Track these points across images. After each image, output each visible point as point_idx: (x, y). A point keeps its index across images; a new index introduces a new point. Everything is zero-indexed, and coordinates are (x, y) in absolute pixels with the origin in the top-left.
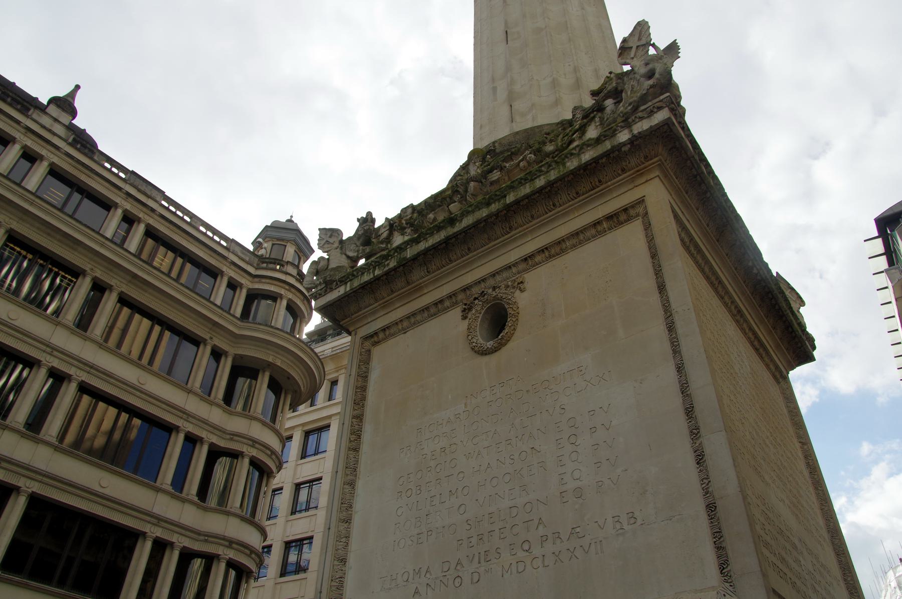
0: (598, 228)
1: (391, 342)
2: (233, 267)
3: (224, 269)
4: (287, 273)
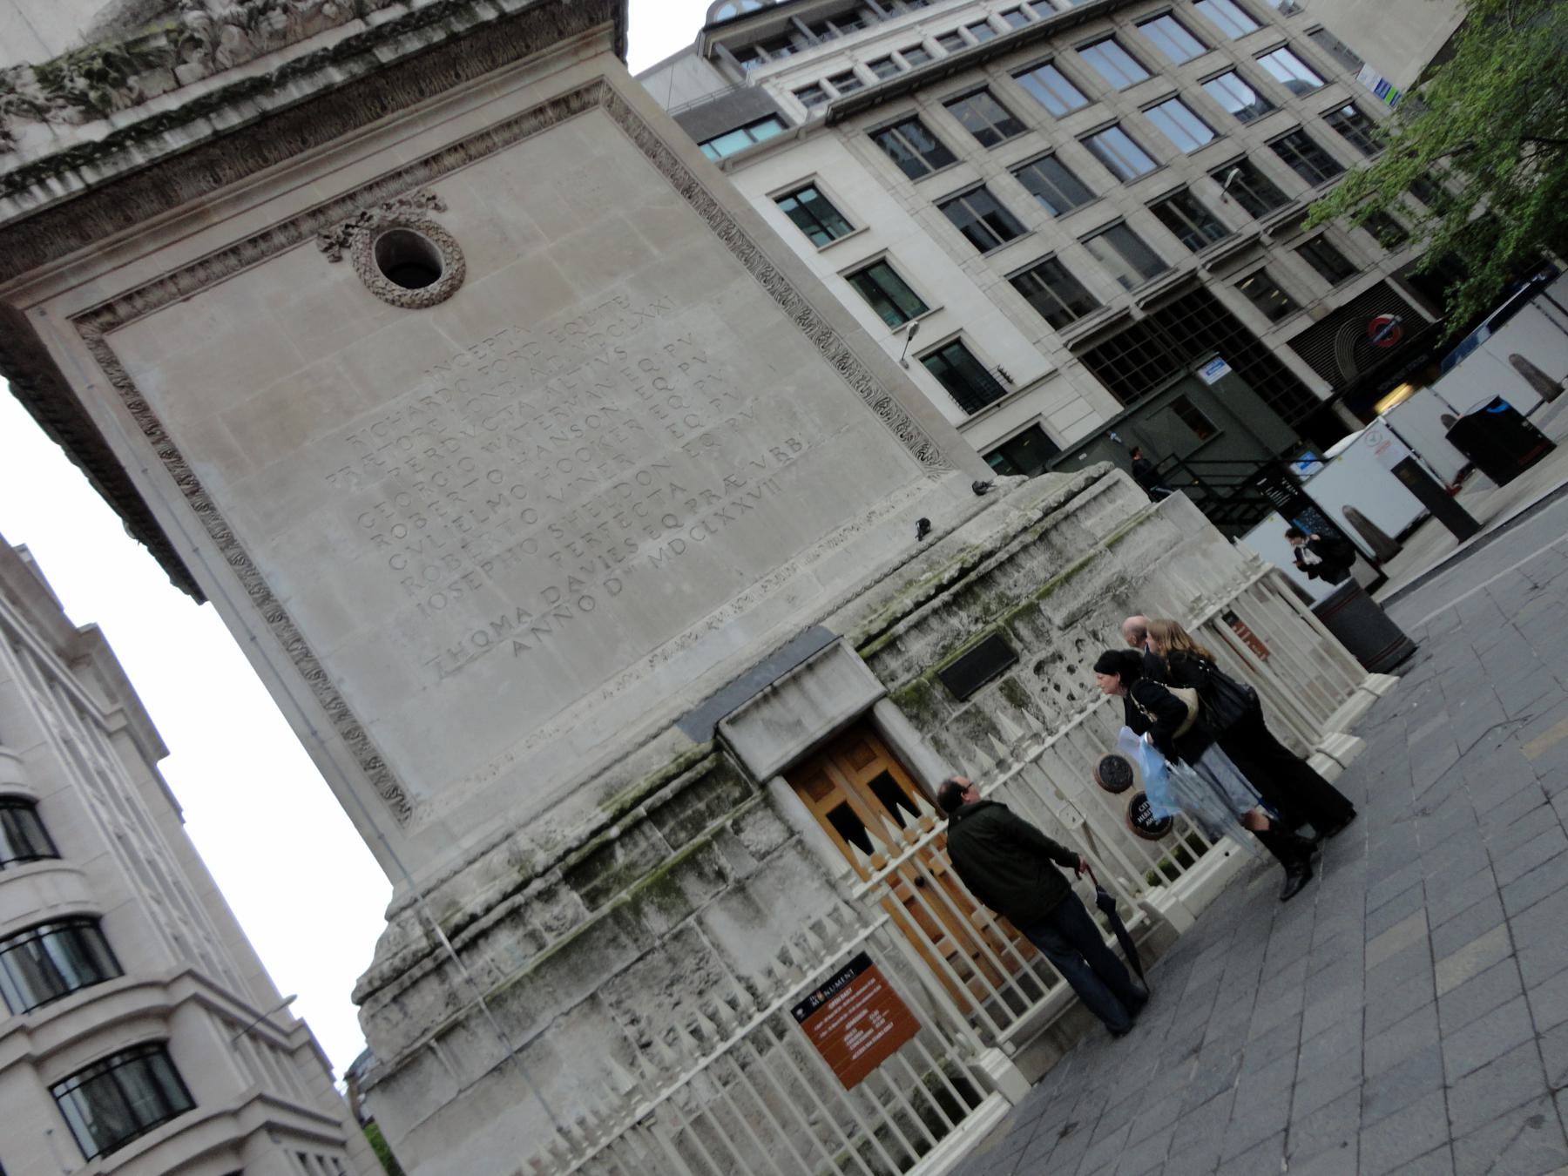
1: (153, 321)
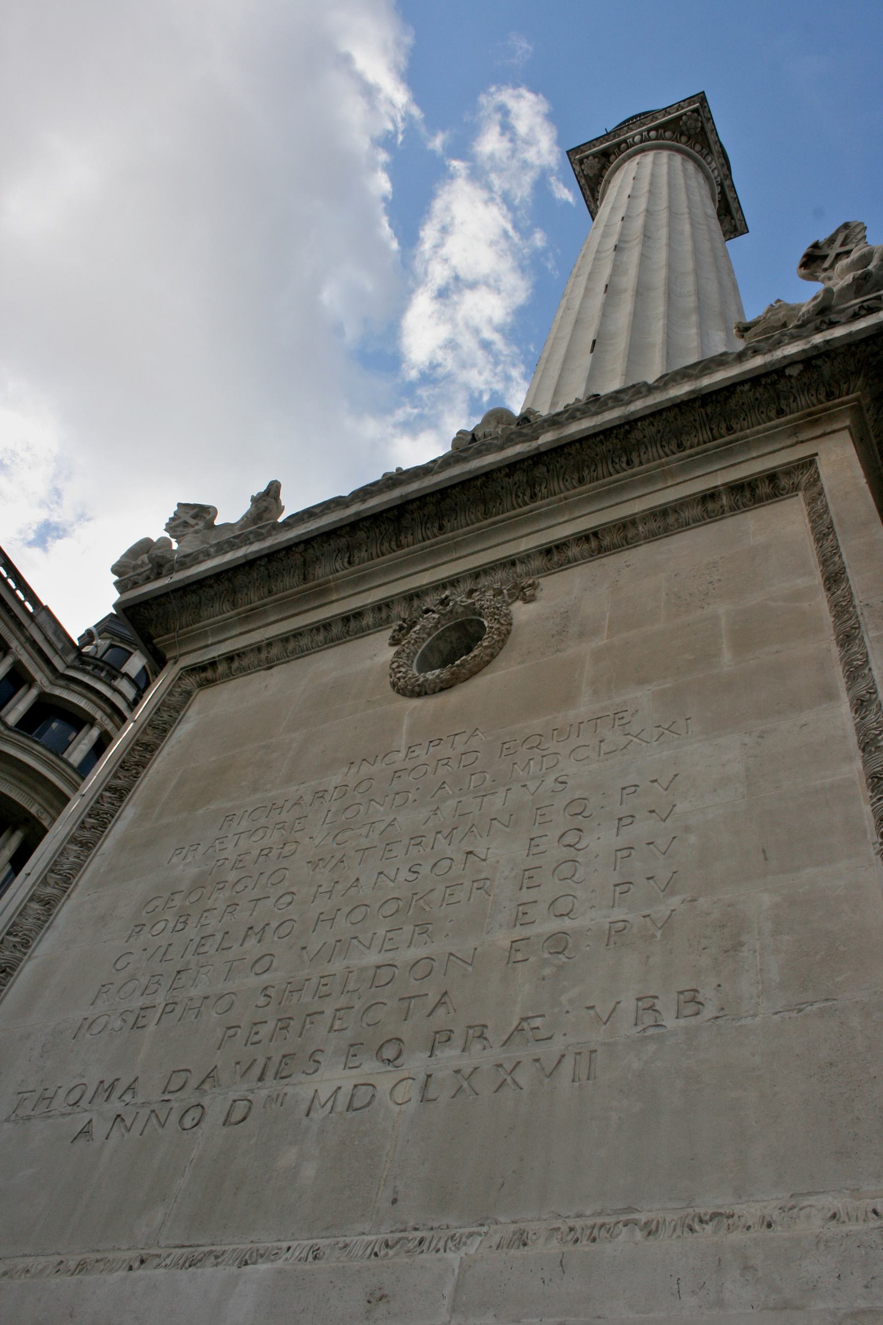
0: (709, 505)
2: (28, 646)
3: (14, 644)
4: (115, 690)
